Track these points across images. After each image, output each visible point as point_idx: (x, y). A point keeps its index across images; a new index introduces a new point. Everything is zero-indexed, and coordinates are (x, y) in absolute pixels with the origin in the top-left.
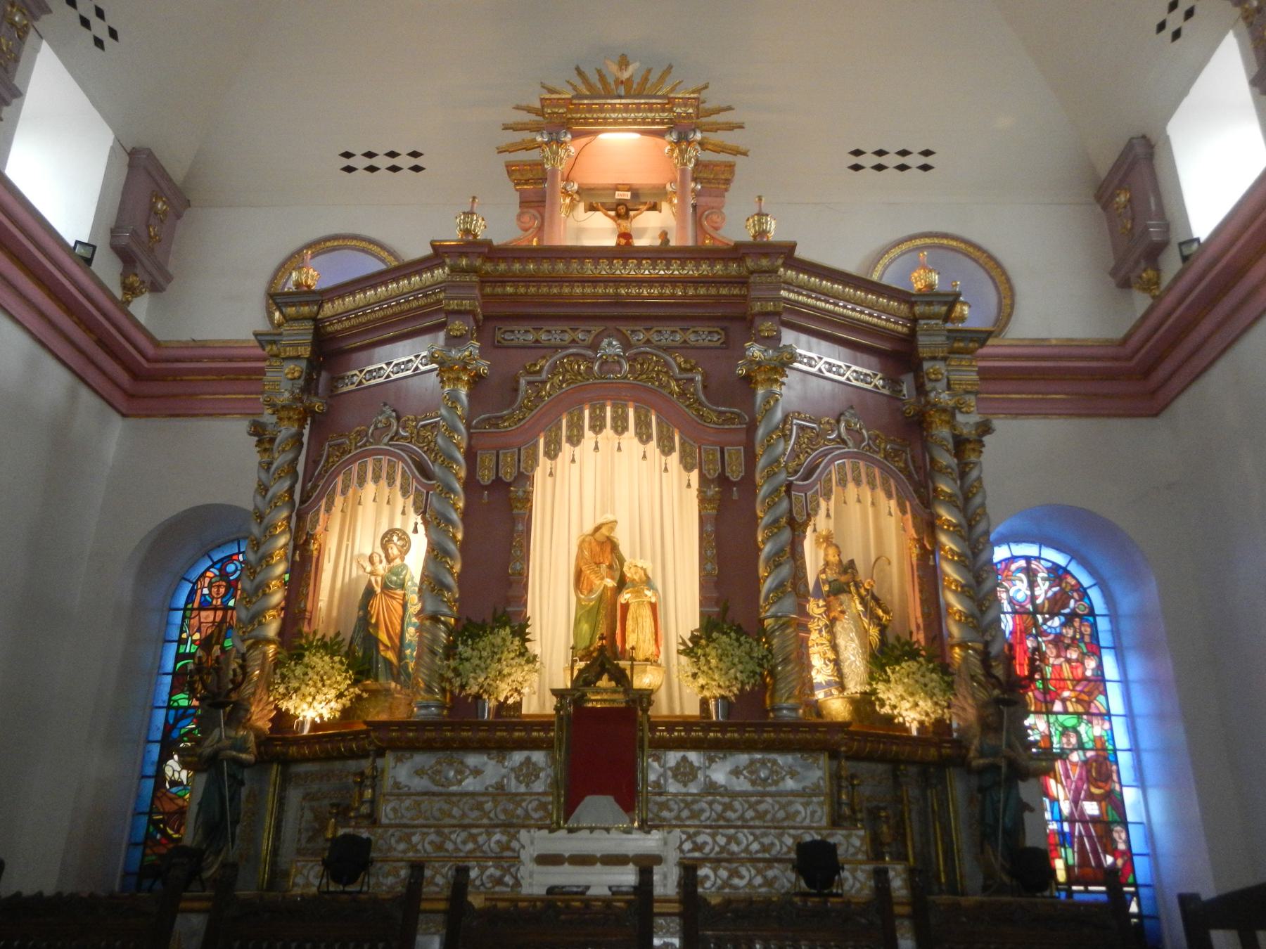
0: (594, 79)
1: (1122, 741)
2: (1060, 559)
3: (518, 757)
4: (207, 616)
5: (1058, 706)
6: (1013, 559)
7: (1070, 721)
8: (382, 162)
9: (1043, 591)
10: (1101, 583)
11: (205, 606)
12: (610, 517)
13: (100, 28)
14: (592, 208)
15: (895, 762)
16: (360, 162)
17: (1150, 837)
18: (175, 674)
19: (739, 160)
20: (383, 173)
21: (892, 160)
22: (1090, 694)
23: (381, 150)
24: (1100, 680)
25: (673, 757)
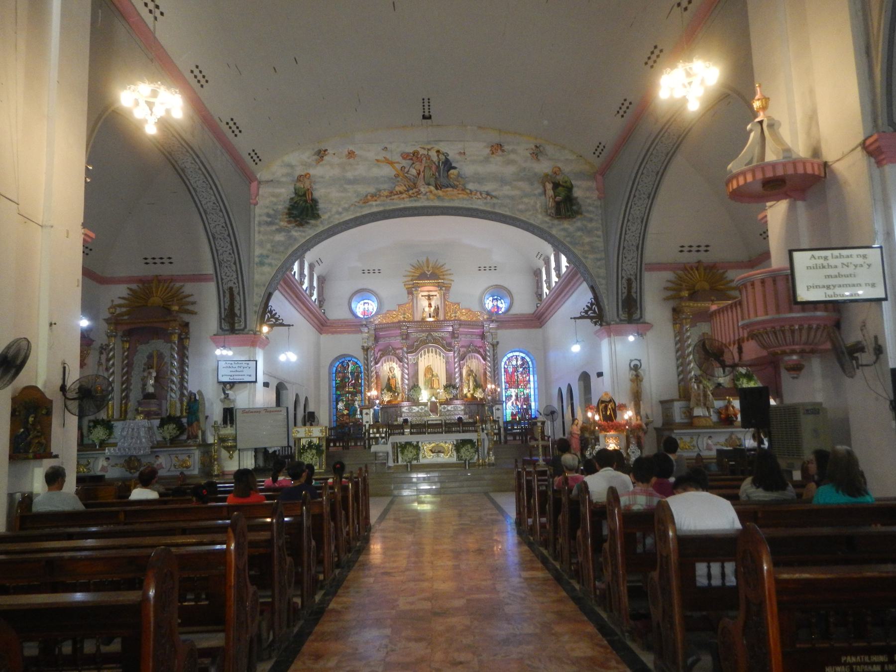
0: (421, 262)
2: (523, 355)
3: (420, 407)
4: (341, 375)
5: (520, 387)
7: (522, 390)
9: (520, 362)
10: (532, 361)
11: (340, 372)
12: (430, 364)
14: (422, 296)
15: (478, 405)
22: (527, 384)
24: (529, 381)
25: (442, 406)
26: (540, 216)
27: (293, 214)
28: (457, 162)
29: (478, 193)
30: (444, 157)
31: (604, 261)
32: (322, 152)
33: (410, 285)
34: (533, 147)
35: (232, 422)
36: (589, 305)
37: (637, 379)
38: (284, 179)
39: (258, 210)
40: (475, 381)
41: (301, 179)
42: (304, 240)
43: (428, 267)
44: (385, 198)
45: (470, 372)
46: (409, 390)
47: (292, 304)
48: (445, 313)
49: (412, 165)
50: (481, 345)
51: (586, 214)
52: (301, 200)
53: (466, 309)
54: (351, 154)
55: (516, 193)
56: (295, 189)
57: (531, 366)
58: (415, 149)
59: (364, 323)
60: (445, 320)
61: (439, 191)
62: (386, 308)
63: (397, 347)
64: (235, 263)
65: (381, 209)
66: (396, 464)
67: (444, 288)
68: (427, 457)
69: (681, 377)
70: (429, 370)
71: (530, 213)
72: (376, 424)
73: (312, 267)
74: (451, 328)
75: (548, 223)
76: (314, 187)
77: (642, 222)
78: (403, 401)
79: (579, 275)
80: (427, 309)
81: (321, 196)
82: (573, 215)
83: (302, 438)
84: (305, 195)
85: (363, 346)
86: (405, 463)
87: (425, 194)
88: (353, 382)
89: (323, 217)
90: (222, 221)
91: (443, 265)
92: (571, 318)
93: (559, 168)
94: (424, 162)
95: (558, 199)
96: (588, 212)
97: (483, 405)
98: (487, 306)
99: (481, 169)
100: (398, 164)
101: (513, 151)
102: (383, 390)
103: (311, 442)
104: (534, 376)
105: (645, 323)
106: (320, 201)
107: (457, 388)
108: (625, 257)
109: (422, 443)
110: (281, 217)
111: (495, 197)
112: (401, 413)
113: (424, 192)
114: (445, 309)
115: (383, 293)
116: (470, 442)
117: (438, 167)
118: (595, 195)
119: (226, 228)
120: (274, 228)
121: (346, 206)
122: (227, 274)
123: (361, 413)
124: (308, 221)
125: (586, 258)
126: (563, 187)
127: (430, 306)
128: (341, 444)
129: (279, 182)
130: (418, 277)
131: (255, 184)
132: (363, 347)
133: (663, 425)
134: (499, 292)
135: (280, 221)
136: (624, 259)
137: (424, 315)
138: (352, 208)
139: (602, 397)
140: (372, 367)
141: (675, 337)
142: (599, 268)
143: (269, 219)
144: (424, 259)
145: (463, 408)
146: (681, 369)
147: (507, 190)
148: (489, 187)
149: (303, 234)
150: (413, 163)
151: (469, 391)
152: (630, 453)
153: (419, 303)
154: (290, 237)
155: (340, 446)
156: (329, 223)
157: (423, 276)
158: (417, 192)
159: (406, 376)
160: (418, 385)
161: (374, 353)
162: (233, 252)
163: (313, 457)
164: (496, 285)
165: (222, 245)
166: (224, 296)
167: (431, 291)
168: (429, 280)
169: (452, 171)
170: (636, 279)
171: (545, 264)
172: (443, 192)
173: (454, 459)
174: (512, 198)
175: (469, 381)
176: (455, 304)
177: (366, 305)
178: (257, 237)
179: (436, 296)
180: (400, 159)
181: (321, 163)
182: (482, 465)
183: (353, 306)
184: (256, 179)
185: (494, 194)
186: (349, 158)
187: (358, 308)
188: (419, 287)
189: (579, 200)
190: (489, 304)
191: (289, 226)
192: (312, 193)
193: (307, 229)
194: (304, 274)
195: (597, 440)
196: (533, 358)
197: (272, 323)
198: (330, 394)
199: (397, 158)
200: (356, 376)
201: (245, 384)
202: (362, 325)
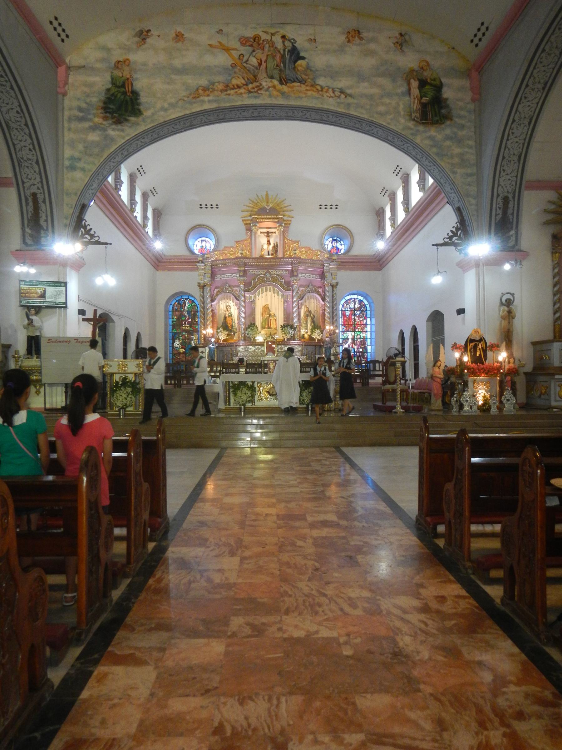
0: (260, 197)
1: (369, 336)
2: (361, 298)
3: (257, 347)
4: (177, 313)
5: (357, 330)
6: (351, 299)
7: (359, 333)
8: (209, 206)
9: (357, 305)
10: (369, 304)
11: (176, 310)
13: (155, 194)
14: (261, 233)
16: (204, 206)
17: (371, 355)
18: (172, 325)
19: (292, 219)
20: (209, 209)
21: (329, 207)
22: (364, 327)
23: (209, 204)
24: (366, 325)
25: (279, 346)
26: (402, 121)
27: (109, 108)
28: (306, 51)
29: (330, 90)
30: (291, 45)
31: (475, 177)
32: (145, 33)
33: (248, 220)
34: (397, 35)
35: (38, 353)
36: (454, 230)
37: (509, 315)
38: (98, 65)
39: (67, 102)
40: (313, 322)
41: (119, 65)
42: (124, 141)
43: (267, 202)
44: (220, 93)
45: (309, 313)
46: (246, 329)
47: (119, 229)
48: (284, 252)
49: (252, 53)
50: (319, 284)
51: (457, 120)
52: (119, 92)
53: (305, 248)
54: (179, 37)
55: (375, 91)
56: (112, 79)
57: (368, 309)
58: (256, 33)
59: (201, 259)
60: (283, 258)
61: (284, 86)
62: (223, 244)
63: (234, 284)
64: (37, 163)
65: (214, 106)
66: (227, 406)
69: (558, 315)
70: (266, 309)
71: (391, 116)
73: (145, 196)
74: (290, 266)
75: (411, 129)
76: (135, 76)
77: (530, 123)
78: (239, 341)
79: (443, 195)
80: (265, 247)
81: (143, 87)
82: (441, 120)
83: (116, 373)
84: (123, 86)
85: (199, 283)
86: (238, 406)
87: (267, 90)
88: (190, 320)
89: (144, 113)
90: (16, 104)
91: (284, 200)
92: (433, 245)
93: (427, 62)
94: (266, 49)
95: (425, 100)
96: (460, 117)
97: (321, 347)
98: (326, 246)
99: (334, 61)
100: (235, 51)
101: (373, 40)
102: (219, 328)
103: (125, 378)
104: (371, 320)
105: (520, 250)
106: (142, 94)
107: (295, 329)
108: (504, 170)
109: (258, 383)
110: (95, 111)
111: (351, 96)
112: (238, 352)
113: (266, 87)
114: (284, 248)
115: (220, 230)
117: (283, 56)
118: (468, 96)
119: (22, 115)
120: (87, 125)
121: (173, 101)
122: (29, 177)
124: (128, 118)
125: (454, 173)
126: (431, 84)
128: (173, 382)
129: (93, 69)
130: (257, 212)
131: (61, 70)
132: (199, 285)
133: (535, 368)
135: (95, 117)
136: (502, 172)
137: (263, 253)
138: (180, 103)
139: (471, 335)
140: (207, 304)
141: (554, 269)
142: (469, 185)
143: (81, 114)
144: (264, 194)
145: (300, 349)
146: (557, 306)
147: (364, 88)
148: (343, 83)
149: (122, 133)
150: (254, 51)
151: (307, 333)
152: (505, 402)
153: (257, 240)
154: (106, 137)
155: (171, 384)
156: (152, 121)
157: (262, 211)
158: (257, 87)
159: (243, 315)
160: (254, 324)
161: (210, 290)
162: (34, 148)
163: (128, 396)
164: (337, 225)
165: (19, 138)
166: (27, 204)
167: (270, 228)
168: (269, 215)
169: (299, 62)
170: (514, 197)
171: (390, 200)
172: (289, 87)
174: (371, 97)
175: (307, 321)
176: (295, 242)
177: (204, 243)
178: (68, 136)
179: (275, 233)
180: (237, 45)
181: (143, 47)
182: (328, 410)
183: (190, 242)
184: (64, 62)
185: (349, 91)
186: (176, 42)
187: (195, 246)
188: (258, 222)
189: (448, 102)
190: (329, 245)
191: (104, 123)
192: (132, 84)
193: (126, 128)
194: (135, 200)
195: (466, 384)
196: (371, 301)
197: (86, 240)
198: (166, 332)
199: (234, 44)
200: (193, 314)
201: (54, 310)
202: (198, 262)
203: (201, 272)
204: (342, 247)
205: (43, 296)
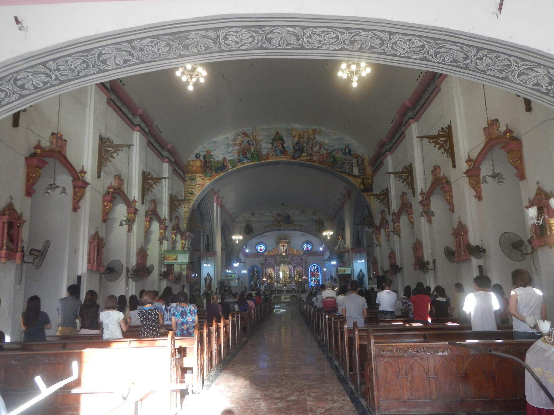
1: (320, 279)
9: (316, 268)
40: (299, 275)
45: (297, 272)
46: (277, 279)
48: (289, 252)
54: (262, 214)
60: (289, 255)
67: (289, 243)
68: (284, 300)
72: (266, 289)
80: (283, 250)
97: (302, 284)
111: (302, 226)
116: (295, 296)
117: (286, 218)
123: (260, 286)
127: (284, 249)
131: (235, 223)
134: (308, 243)
157: (281, 239)
173: (290, 301)
200: (258, 272)
203: (261, 259)
204: (310, 247)
205: (231, 276)
